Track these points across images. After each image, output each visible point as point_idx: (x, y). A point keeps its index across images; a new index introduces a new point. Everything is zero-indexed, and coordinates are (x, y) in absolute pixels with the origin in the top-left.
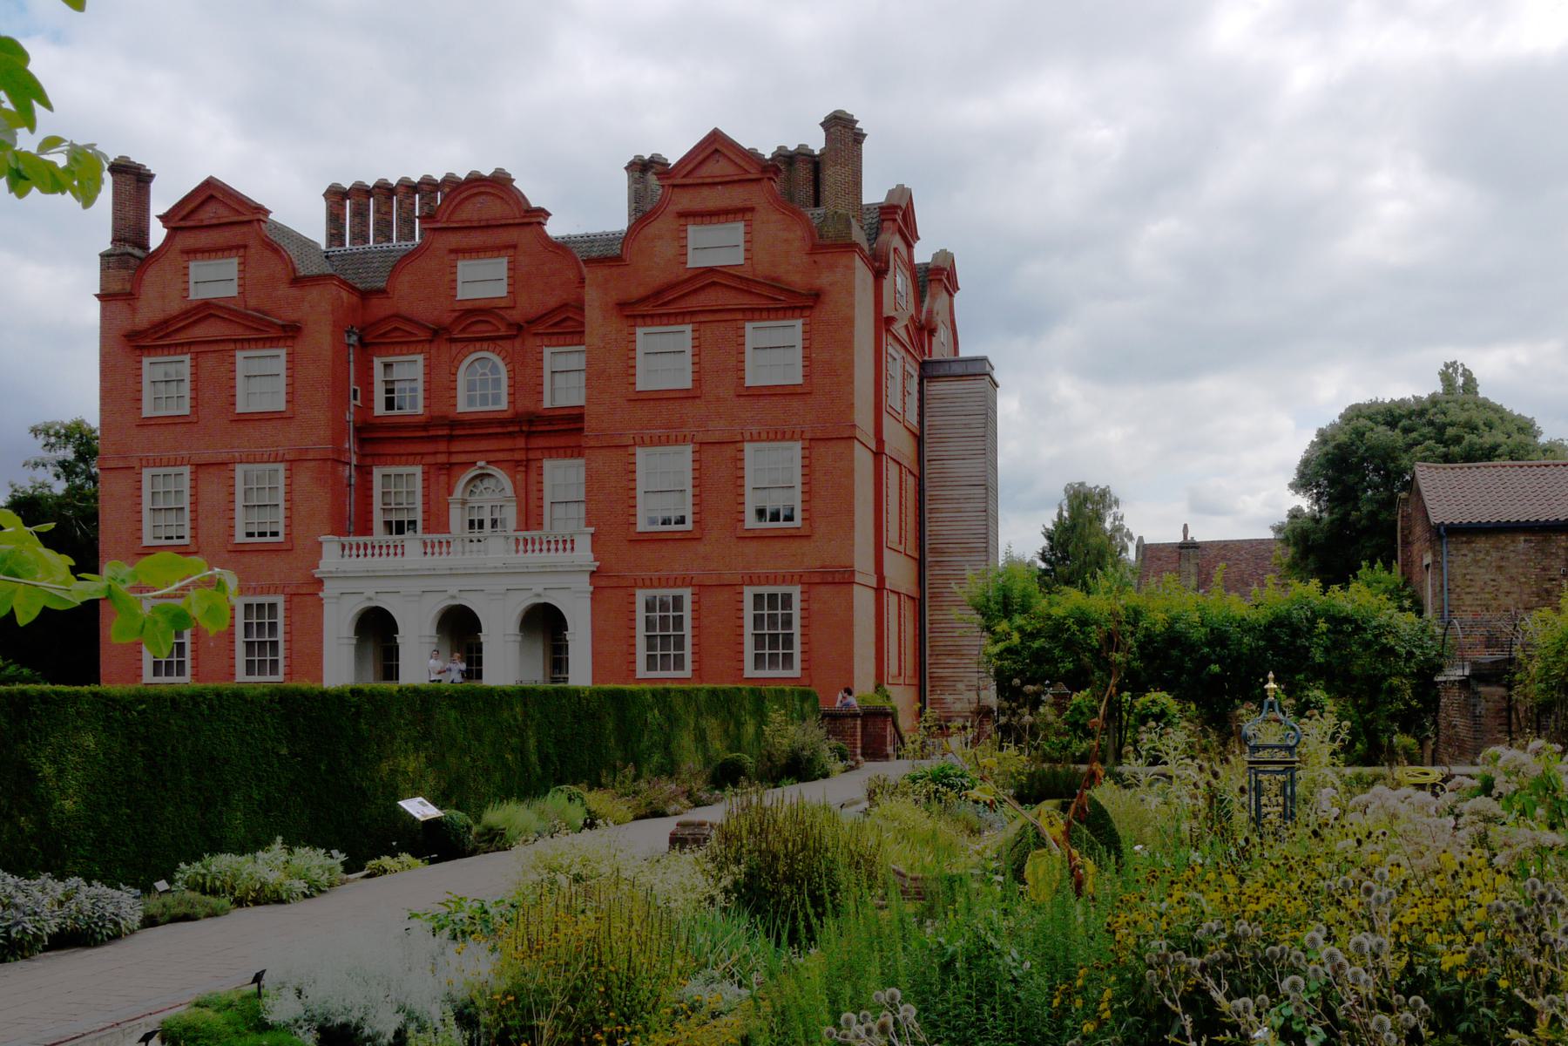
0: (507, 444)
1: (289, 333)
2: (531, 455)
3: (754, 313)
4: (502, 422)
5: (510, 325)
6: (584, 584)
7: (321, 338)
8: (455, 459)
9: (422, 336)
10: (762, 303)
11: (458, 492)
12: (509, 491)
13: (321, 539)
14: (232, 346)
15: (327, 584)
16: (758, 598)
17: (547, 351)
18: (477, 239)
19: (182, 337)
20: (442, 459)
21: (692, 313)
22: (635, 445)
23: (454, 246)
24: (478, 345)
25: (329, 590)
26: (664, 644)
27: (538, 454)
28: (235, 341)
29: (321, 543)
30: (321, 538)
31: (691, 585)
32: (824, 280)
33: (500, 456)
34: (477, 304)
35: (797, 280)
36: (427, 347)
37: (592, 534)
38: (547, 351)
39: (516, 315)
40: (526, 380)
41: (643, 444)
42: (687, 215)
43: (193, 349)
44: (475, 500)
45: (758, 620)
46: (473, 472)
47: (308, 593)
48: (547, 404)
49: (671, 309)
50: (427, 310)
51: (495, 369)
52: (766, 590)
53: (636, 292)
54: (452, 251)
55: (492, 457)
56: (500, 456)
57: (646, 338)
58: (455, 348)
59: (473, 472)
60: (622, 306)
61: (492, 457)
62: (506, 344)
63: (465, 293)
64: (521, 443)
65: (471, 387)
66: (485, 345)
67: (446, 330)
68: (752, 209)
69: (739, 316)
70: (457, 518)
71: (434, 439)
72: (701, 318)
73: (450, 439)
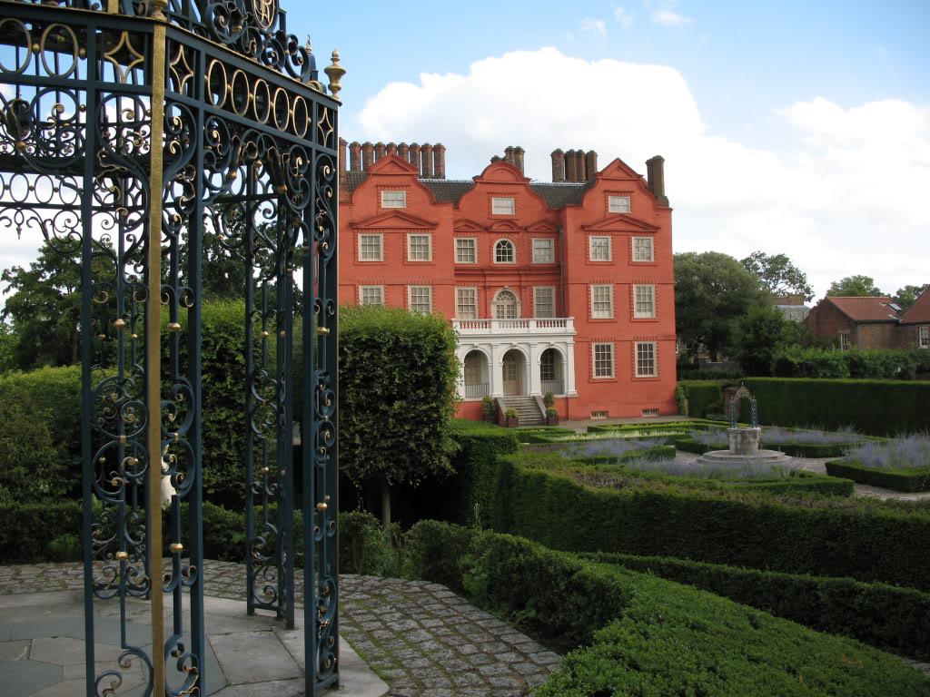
0: (517, 278)
1: (432, 226)
3: (635, 233)
4: (518, 269)
5: (520, 228)
6: (570, 340)
7: (446, 226)
8: (494, 284)
9: (478, 229)
10: (642, 230)
11: (495, 300)
12: (518, 300)
18: (499, 189)
19: (380, 225)
20: (488, 284)
23: (489, 191)
26: (604, 365)
27: (530, 283)
32: (660, 222)
33: (515, 284)
34: (505, 218)
35: (650, 221)
36: (479, 234)
38: (533, 240)
39: (519, 223)
41: (593, 283)
43: (386, 231)
45: (640, 354)
46: (500, 290)
48: (534, 262)
49: (606, 228)
50: (482, 220)
51: (509, 246)
52: (643, 343)
53: (589, 221)
54: (488, 193)
55: (511, 284)
56: (515, 284)
57: (593, 240)
58: (493, 236)
59: (500, 290)
60: (583, 227)
61: (511, 284)
62: (516, 236)
63: (495, 211)
64: (523, 278)
65: (498, 252)
68: (631, 192)
69: (630, 233)
70: (493, 310)
71: (484, 276)
73: (492, 275)
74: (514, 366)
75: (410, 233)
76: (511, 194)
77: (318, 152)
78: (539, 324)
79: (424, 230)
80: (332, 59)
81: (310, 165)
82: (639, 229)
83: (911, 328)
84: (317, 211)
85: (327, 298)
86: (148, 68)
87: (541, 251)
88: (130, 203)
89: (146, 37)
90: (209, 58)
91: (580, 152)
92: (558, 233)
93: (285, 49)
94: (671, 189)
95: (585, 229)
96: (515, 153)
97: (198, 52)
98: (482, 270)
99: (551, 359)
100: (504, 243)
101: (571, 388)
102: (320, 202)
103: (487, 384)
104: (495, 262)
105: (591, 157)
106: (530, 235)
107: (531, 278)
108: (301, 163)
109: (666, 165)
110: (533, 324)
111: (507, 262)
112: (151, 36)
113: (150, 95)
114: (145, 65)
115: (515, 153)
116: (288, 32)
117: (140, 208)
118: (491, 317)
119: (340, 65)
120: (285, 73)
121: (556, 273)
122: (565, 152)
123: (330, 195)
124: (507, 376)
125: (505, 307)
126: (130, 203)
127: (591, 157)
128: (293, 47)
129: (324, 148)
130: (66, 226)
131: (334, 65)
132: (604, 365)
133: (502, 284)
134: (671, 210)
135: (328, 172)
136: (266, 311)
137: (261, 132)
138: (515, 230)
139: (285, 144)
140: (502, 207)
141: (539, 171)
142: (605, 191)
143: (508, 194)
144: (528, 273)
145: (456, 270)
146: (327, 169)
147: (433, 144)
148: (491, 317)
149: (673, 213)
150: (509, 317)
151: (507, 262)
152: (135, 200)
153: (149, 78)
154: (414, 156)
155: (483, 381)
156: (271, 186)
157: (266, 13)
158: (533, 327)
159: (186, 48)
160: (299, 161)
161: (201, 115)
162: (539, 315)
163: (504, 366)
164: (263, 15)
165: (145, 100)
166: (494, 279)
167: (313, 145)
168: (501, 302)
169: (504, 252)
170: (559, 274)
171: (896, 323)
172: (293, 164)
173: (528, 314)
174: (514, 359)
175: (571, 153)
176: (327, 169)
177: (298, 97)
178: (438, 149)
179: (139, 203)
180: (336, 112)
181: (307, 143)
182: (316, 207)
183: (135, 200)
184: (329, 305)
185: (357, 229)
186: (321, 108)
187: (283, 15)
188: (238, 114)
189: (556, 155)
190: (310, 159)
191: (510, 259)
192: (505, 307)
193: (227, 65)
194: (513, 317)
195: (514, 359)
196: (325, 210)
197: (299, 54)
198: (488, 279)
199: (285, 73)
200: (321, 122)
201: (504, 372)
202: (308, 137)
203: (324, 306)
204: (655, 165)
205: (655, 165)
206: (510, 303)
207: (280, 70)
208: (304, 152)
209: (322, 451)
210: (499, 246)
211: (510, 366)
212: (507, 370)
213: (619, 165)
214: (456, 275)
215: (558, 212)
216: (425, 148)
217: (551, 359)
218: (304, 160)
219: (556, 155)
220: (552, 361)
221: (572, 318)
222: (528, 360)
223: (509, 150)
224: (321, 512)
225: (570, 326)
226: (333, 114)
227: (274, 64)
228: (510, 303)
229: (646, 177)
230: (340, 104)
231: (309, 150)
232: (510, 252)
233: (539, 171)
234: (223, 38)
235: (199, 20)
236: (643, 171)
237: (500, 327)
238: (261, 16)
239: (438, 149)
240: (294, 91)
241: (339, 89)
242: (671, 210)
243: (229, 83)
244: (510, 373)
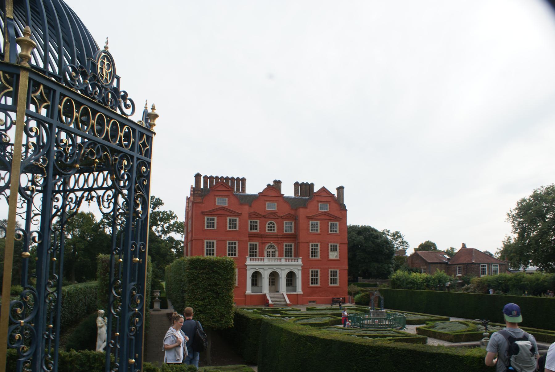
0: (277, 239)
1: (239, 215)
2: (282, 242)
6: (300, 268)
10: (333, 219)
12: (277, 249)
13: (247, 257)
14: (226, 216)
15: (247, 266)
16: (331, 271)
17: (285, 222)
20: (263, 241)
21: (320, 219)
22: (310, 242)
24: (271, 219)
25: (248, 267)
28: (227, 215)
29: (246, 258)
30: (247, 257)
31: (320, 269)
37: (302, 259)
39: (279, 215)
40: (280, 228)
41: (311, 242)
42: (318, 201)
43: (218, 216)
44: (269, 250)
46: (270, 244)
47: (244, 268)
51: (273, 224)
54: (265, 200)
58: (266, 219)
60: (307, 217)
62: (276, 219)
64: (280, 239)
65: (268, 227)
66: (272, 219)
67: (265, 216)
70: (266, 253)
71: (262, 237)
72: (321, 220)
74: (274, 279)
75: (229, 217)
76: (275, 201)
77: (138, 159)
78: (286, 260)
79: (235, 216)
80: (151, 109)
81: (132, 166)
82: (333, 219)
83: (453, 266)
84: (136, 192)
85: (141, 241)
86: (15, 95)
87: (288, 227)
88: (57, 189)
89: (15, 76)
90: (63, 96)
91: (307, 183)
92: (296, 219)
93: (119, 98)
94: (347, 201)
95: (309, 218)
96: (278, 183)
97: (55, 91)
98: (261, 235)
99: (291, 276)
100: (271, 223)
101: (299, 291)
102: (138, 187)
103: (262, 287)
104: (267, 231)
105: (312, 185)
106: (283, 219)
107: (282, 239)
108: (126, 163)
109: (345, 190)
110: (283, 260)
111: (272, 232)
112: (18, 76)
113: (15, 111)
114: (13, 94)
115: (278, 183)
116: (121, 89)
117: (61, 191)
118: (264, 257)
119: (156, 112)
120: (119, 112)
121: (294, 237)
122: (300, 183)
123: (145, 183)
124: (271, 283)
125: (271, 252)
126: (57, 189)
127: (312, 185)
128: (125, 97)
129: (143, 157)
130: (21, 199)
131: (152, 111)
132: (314, 281)
133: (269, 241)
134: (347, 210)
135: (145, 170)
136: (121, 249)
137: (99, 143)
138: (277, 217)
139: (114, 151)
140: (271, 207)
141: (288, 191)
142: (318, 201)
143: (275, 201)
144: (280, 237)
145: (249, 234)
146: (144, 169)
147: (241, 177)
148: (264, 257)
149: (347, 211)
150: (272, 257)
151: (272, 232)
152: (59, 187)
153: (15, 102)
154: (233, 183)
155: (260, 285)
156: (127, 181)
157: (107, 76)
158: (283, 262)
159: (45, 87)
160: (125, 162)
161: (135, 159)
162: (286, 256)
163: (269, 279)
164: (105, 77)
165: (13, 115)
166: (266, 239)
167: (136, 154)
168: (269, 250)
169: (271, 228)
170: (296, 238)
171: (447, 263)
172: (121, 163)
173: (281, 255)
174: (274, 276)
175: (303, 184)
176: (144, 169)
177: (99, 114)
178: (244, 180)
179: (61, 189)
180: (152, 138)
181: (131, 153)
182: (135, 189)
183: (59, 187)
184: (141, 246)
185: (205, 214)
186: (142, 135)
187: (118, 79)
188: (112, 143)
189: (296, 184)
190: (133, 162)
191: (274, 230)
192: (271, 252)
193: (76, 102)
194: (274, 257)
195: (274, 276)
196: (142, 192)
197: (128, 102)
198: (263, 239)
199: (119, 112)
200: (142, 142)
201: (269, 282)
202: (132, 149)
203: (138, 246)
204: (340, 189)
205: (340, 189)
206: (273, 250)
207: (116, 110)
208: (130, 158)
209: (133, 330)
210: (269, 224)
211: (272, 279)
212: (271, 281)
213: (324, 189)
214: (249, 237)
215: (296, 210)
216: (238, 179)
217: (291, 276)
218: (128, 162)
219: (296, 184)
220: (291, 277)
221: (301, 258)
222: (280, 276)
223: (275, 182)
224: (130, 365)
225: (300, 262)
226: (149, 139)
227: (111, 106)
228: (273, 250)
229: (336, 195)
230: (155, 134)
231: (132, 157)
232: (274, 227)
233: (288, 191)
234: (74, 85)
235: (58, 74)
236: (334, 192)
237: (268, 261)
238: (103, 77)
239: (244, 180)
240: (125, 123)
241: (155, 125)
242: (347, 210)
243: (77, 112)
244: (272, 282)
